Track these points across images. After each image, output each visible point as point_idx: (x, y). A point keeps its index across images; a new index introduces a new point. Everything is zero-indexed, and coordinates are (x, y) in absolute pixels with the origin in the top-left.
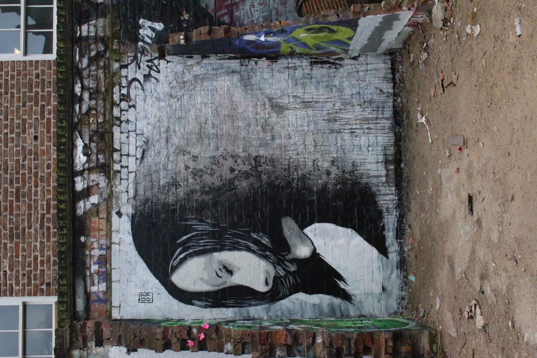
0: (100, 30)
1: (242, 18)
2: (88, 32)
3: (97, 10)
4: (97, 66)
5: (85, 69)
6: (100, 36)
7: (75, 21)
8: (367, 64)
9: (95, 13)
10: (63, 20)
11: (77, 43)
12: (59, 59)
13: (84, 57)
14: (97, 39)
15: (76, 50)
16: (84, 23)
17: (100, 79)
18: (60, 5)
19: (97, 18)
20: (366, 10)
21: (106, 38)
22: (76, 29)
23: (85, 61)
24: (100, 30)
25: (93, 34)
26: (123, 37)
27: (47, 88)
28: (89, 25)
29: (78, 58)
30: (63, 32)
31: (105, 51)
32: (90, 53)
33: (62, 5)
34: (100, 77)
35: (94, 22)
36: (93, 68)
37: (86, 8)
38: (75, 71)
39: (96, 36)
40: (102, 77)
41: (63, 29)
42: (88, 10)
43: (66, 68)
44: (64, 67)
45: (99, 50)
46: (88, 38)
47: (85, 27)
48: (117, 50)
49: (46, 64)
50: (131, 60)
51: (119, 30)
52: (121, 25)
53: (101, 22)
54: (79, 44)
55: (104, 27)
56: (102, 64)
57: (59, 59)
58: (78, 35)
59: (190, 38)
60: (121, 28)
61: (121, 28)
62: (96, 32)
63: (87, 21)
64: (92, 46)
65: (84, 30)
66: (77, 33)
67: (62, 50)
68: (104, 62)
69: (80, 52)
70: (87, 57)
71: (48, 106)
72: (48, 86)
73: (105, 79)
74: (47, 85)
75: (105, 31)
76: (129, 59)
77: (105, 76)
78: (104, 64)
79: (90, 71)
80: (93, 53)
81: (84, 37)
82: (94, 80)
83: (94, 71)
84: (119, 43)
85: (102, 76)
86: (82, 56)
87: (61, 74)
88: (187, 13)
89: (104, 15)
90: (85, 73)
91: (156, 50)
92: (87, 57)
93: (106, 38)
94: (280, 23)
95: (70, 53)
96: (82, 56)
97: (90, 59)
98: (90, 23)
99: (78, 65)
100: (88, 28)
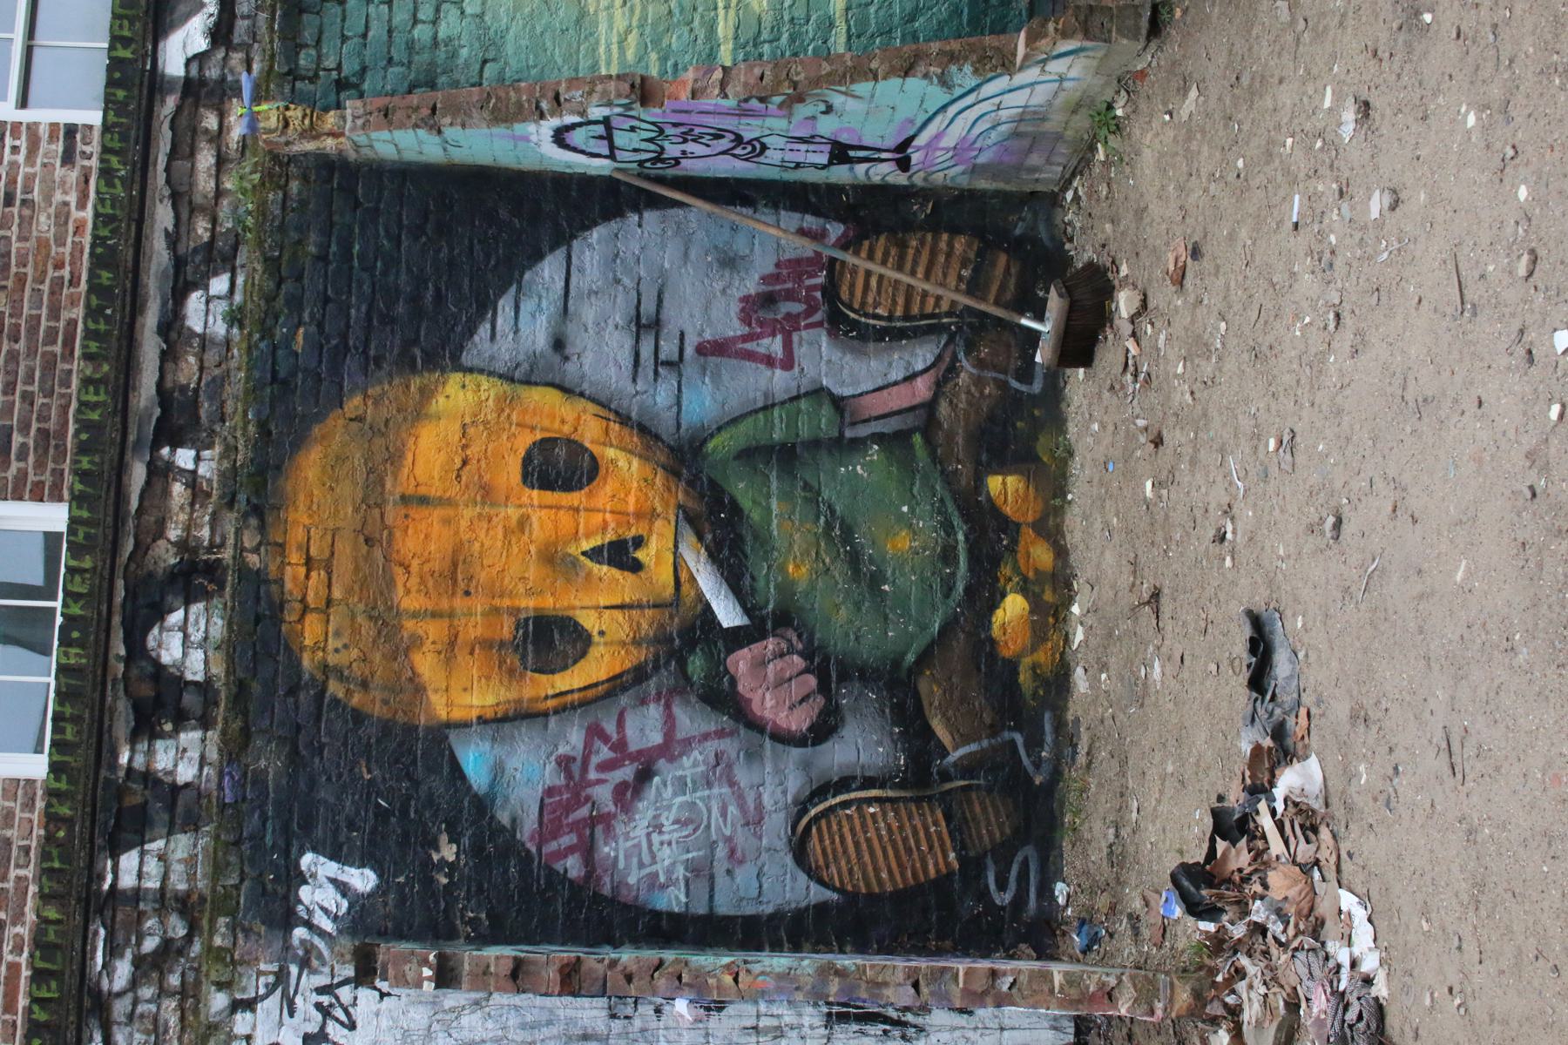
0: (178, 870)
1: (621, 864)
2: (140, 876)
3: (171, 807)
4: (161, 988)
5: (119, 995)
7: (99, 841)
8: (1002, 1029)
9: (166, 817)
10: (61, 834)
11: (100, 911)
12: (42, 958)
13: (122, 956)
14: (164, 900)
15: (96, 933)
17: (166, 1031)
18: (57, 785)
19: (170, 834)
20: (1005, 988)
21: (195, 897)
22: (99, 866)
23: (124, 969)
24: (178, 870)
25: (152, 884)
26: (247, 909)
27: (17, 866)
28: (142, 854)
29: (99, 960)
30: (60, 870)
31: (189, 938)
32: (139, 944)
33: (63, 786)
34: (166, 1022)
35: (160, 844)
36: (147, 992)
37: (138, 799)
38: (87, 1003)
39: (163, 888)
40: (171, 1024)
41: (61, 861)
42: (146, 802)
43: (60, 989)
44: (54, 985)
45: (170, 934)
46: (137, 894)
47: (129, 861)
48: (228, 950)
49: (20, 792)
50: (267, 985)
51: (237, 887)
52: (242, 871)
53: (182, 845)
54: (108, 913)
55: (190, 862)
56: (174, 980)
57: (42, 958)
58: (106, 887)
59: (452, 970)
60: (242, 880)
61: (242, 880)
62: (165, 878)
64: (149, 923)
65: (129, 869)
67: (51, 929)
68: (183, 975)
69: (109, 940)
70: (129, 954)
71: (14, 924)
72: (21, 862)
73: (183, 1029)
74: (17, 858)
75: (191, 877)
76: (262, 980)
77: (182, 1019)
78: (183, 983)
79: (135, 1002)
80: (150, 944)
81: (124, 891)
82: (147, 1033)
83: (149, 1001)
84: (233, 928)
85: (173, 1021)
86: (113, 952)
87: (42, 1008)
88: (450, 842)
89: (192, 824)
90: (120, 1008)
91: (348, 957)
92: (129, 954)
93: (195, 897)
94: (736, 980)
95: (78, 945)
96: (113, 952)
97: (138, 961)
98: (147, 847)
99: (98, 982)
100: (141, 863)
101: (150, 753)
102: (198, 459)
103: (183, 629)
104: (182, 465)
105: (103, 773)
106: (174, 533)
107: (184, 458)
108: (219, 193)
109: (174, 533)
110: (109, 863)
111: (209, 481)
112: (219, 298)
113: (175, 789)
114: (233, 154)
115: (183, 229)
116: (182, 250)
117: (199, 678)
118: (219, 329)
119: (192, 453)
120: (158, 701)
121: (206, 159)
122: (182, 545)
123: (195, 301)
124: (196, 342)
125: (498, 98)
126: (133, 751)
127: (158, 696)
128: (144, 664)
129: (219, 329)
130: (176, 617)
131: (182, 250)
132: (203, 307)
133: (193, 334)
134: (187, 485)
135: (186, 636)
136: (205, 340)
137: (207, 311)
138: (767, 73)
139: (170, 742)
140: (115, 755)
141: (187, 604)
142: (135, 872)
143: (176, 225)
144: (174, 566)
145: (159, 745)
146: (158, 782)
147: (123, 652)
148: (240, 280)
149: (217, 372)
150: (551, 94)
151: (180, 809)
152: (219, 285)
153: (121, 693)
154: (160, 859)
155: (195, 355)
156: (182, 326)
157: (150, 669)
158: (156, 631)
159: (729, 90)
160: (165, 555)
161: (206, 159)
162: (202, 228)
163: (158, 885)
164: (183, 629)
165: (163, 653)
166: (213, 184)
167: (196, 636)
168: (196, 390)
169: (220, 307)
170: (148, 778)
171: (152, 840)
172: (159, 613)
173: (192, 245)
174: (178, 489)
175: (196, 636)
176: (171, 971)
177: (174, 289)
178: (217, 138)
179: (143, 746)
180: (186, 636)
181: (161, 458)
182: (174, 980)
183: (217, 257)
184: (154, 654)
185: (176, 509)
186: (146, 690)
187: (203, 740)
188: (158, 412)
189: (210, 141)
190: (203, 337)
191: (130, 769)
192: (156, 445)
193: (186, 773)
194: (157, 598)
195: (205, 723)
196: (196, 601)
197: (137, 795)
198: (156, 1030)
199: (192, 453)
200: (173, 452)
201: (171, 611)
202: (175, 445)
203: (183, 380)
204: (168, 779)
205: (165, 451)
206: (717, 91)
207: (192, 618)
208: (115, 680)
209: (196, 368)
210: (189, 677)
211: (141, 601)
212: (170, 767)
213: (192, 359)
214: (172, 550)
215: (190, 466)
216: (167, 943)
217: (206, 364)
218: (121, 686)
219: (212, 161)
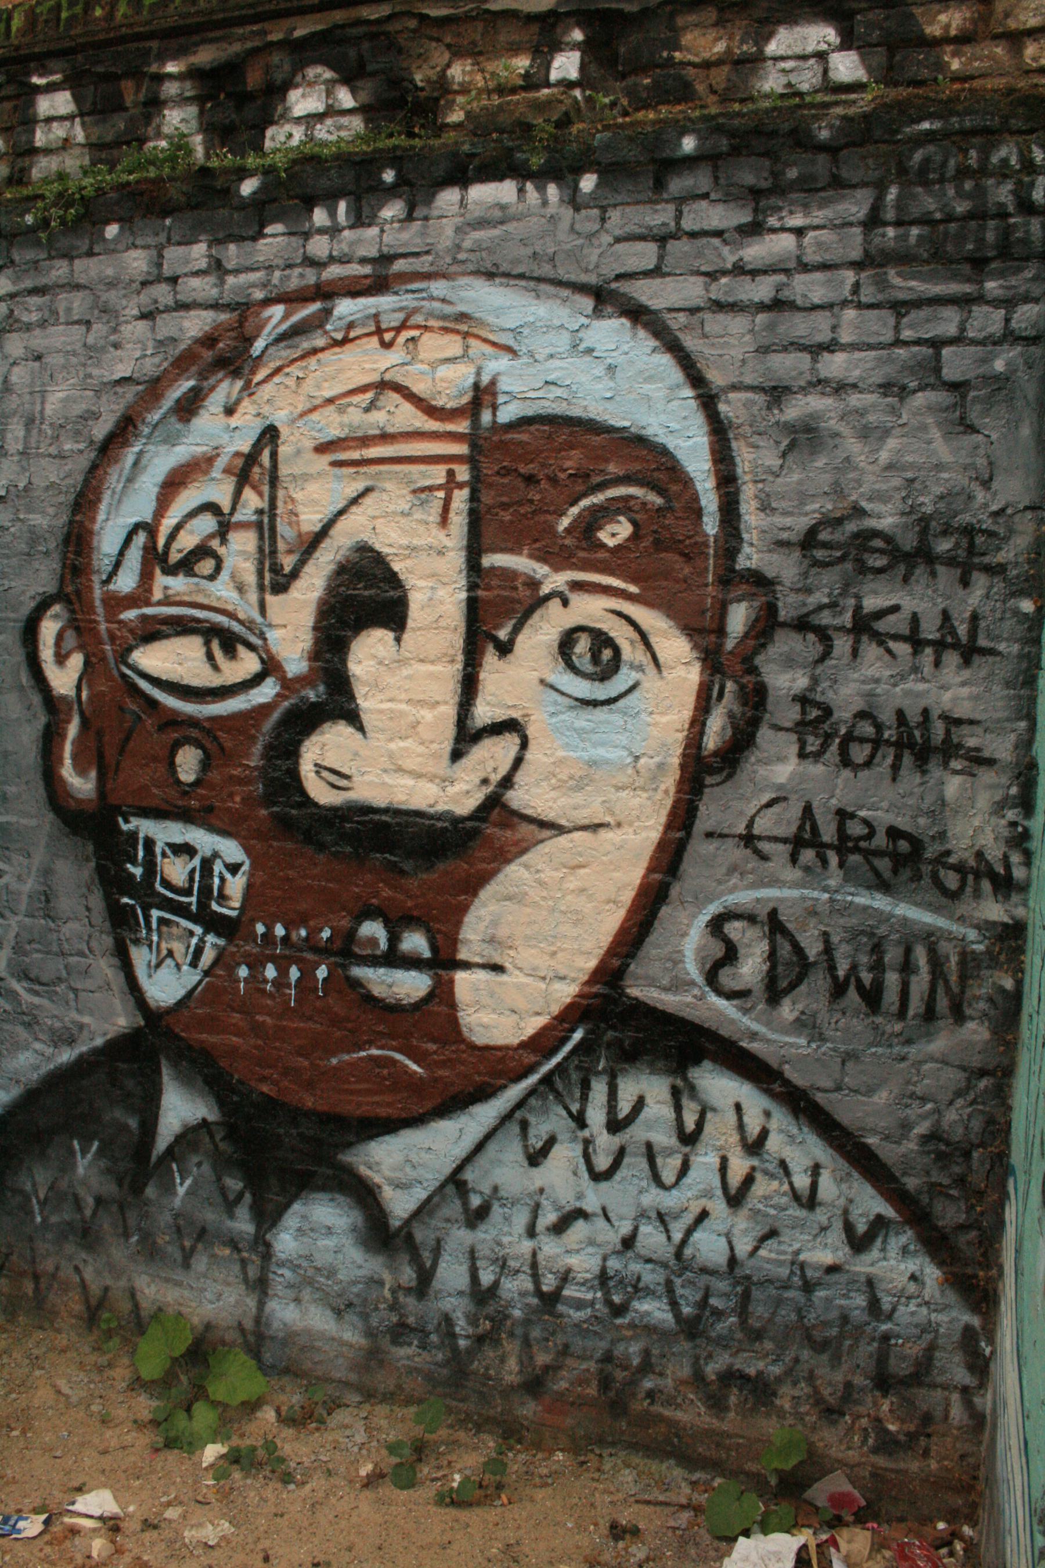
2: (49, 120)
9: (109, 138)
16: (77, 99)
22: (52, 64)
25: (40, 138)
28: (70, 118)
37: (129, 100)
42: (122, 108)
47: (62, 102)
62: (47, 151)
63: (84, 111)
66: (41, 76)
98: (78, 120)
100: (62, 118)
101: (182, 101)
103: (331, 111)
104: (556, 64)
105: (155, 44)
106: (458, 72)
107: (566, 65)
109: (458, 72)
110: (57, 77)
112: (826, 71)
119: (574, 74)
120: (242, 99)
122: (442, 86)
123: (821, 34)
126: (180, 77)
128: (287, 67)
129: (771, 82)
130: (345, 98)
132: (810, 49)
134: (527, 76)
135: (320, 117)
137: (804, 58)
139: (194, 124)
140: (174, 58)
141: (362, 110)
142: (53, 113)
144: (412, 81)
146: (148, 118)
147: (298, 33)
149: (700, 88)
152: (846, 67)
153: (249, 45)
154: (66, 140)
155: (729, 50)
156: (779, 22)
158: (328, 74)
163: (38, 144)
164: (331, 111)
165: (299, 91)
168: (670, 62)
169: (807, 79)
170: (155, 104)
174: (522, 63)
175: (321, 132)
179: (189, 89)
181: (567, 30)
184: (298, 78)
185: (490, 67)
186: (254, 79)
191: (161, 78)
192: (584, 18)
194: (370, 68)
196: (367, 121)
197: (131, 93)
199: (574, 74)
200: (575, 46)
201: (354, 92)
202: (586, 48)
203: (687, 39)
205: (578, 35)
207: (344, 120)
208: (265, 33)
209: (706, 55)
211: (366, 45)
213: (720, 47)
214: (433, 74)
215: (554, 76)
217: (713, 71)
218: (257, 43)
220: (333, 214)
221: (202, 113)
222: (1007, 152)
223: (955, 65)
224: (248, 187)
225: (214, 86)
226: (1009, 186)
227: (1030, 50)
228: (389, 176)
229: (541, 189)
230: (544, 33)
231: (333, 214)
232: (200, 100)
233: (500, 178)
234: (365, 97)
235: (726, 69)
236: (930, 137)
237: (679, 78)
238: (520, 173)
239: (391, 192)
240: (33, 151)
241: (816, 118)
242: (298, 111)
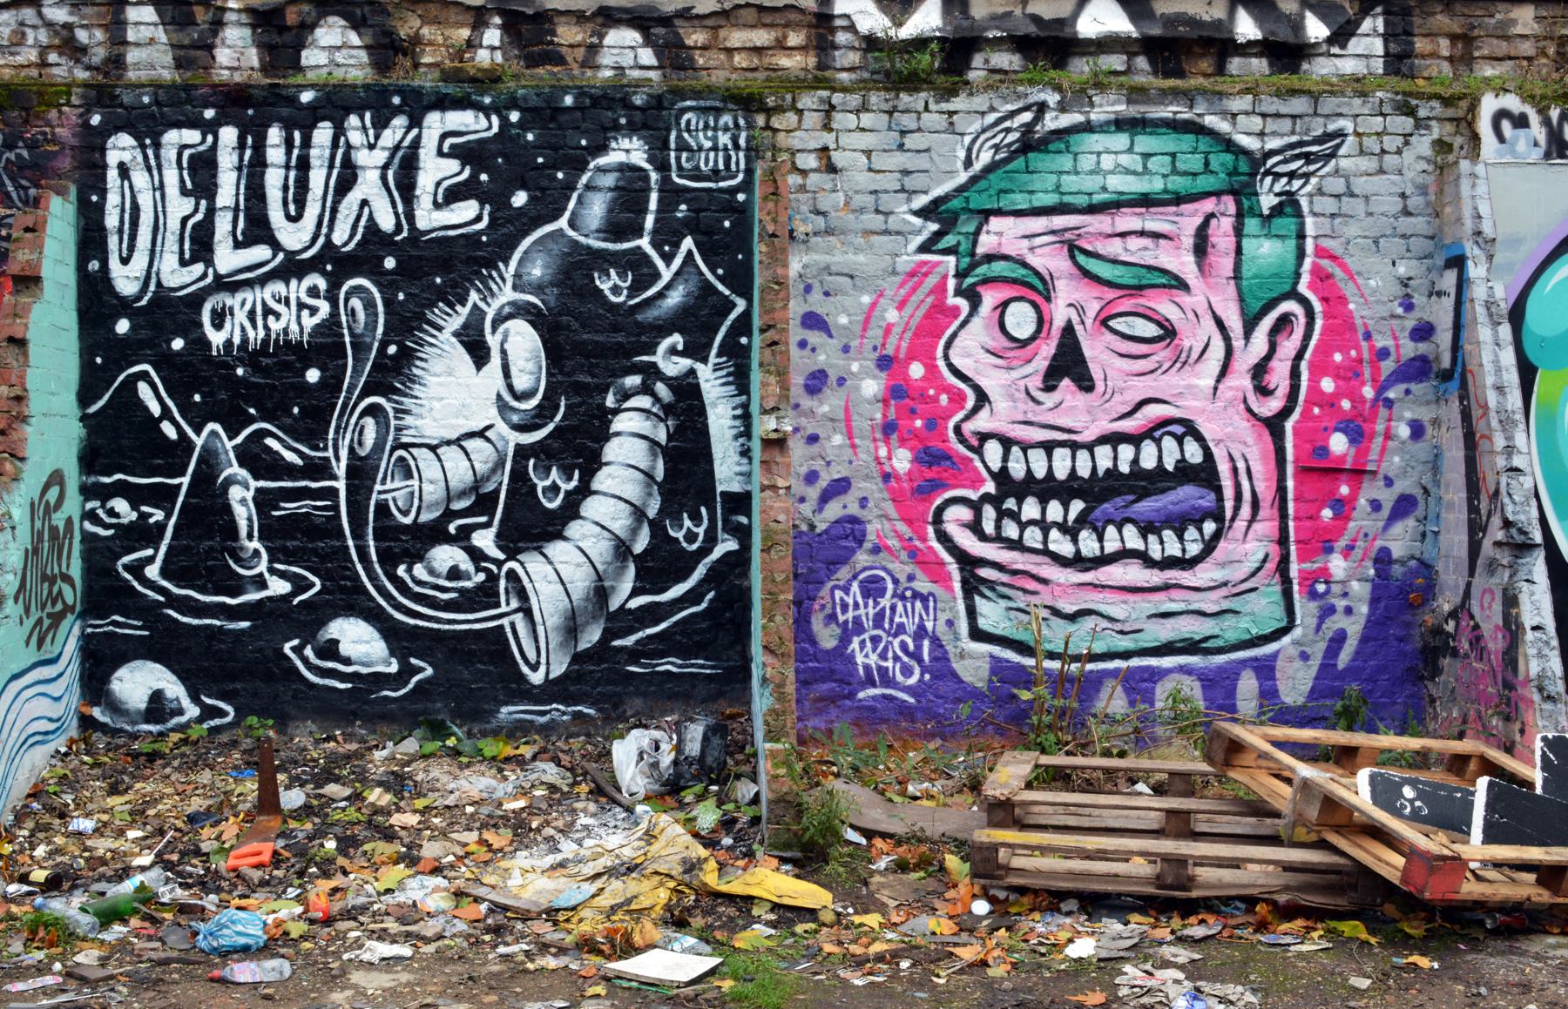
2: (136, 24)
3: (194, 46)
5: (40, 14)
6: (124, 55)
9: (186, 42)
13: (71, 14)
16: (159, 13)
17: (12, 54)
19: (172, 45)
25: (131, 35)
28: (156, 25)
32: (82, 26)
35: (163, 38)
36: (43, 36)
47: (148, 13)
62: (137, 45)
65: (142, 16)
68: (58, 65)
79: (34, 27)
80: (82, 36)
81: (123, 12)
85: (20, 59)
89: (179, 64)
92: (71, 19)
97: (68, 27)
102: (493, 48)
103: (345, 46)
104: (486, 36)
106: (425, 31)
107: (492, 36)
108: (730, 51)
111: (472, 59)
113: (210, 48)
114: (767, 60)
115: (696, 22)
116: (677, 22)
117: (304, 62)
118: (607, 59)
119: (497, 44)
120: (283, 29)
121: (761, 37)
122: (416, 40)
123: (632, 36)
124: (595, 40)
125: (777, 293)
127: (289, 29)
128: (314, 14)
130: (354, 38)
131: (677, 22)
133: (602, 36)
135: (339, 48)
136: (593, 49)
138: (780, 526)
139: (249, 41)
141: (367, 47)
143: (698, 17)
145: (247, 32)
146: (215, 34)
148: (653, 74)
149: (569, 59)
150: (776, 338)
151: (192, 53)
157: (309, 20)
158: (343, 22)
159: (768, 493)
160: (408, 25)
161: (761, 37)
162: (696, 38)
164: (345, 46)
166: (737, 45)
167: (339, 57)
168: (552, 43)
169: (627, 60)
170: (218, 24)
171: (166, 31)
172: (356, 25)
173: (681, 31)
175: (339, 57)
176: (60, 54)
177: (641, 18)
178: (780, 45)
179: (244, 18)
180: (339, 48)
182: (53, 57)
183: (673, 55)
187: (252, 69)
188: (530, 11)
189: (777, 39)
190: (600, 45)
192: (502, 12)
193: (223, 56)
195: (265, 69)
196: (370, 55)
198: (13, 45)
199: (497, 44)
201: (360, 35)
202: (505, 28)
203: (560, 30)
204: (218, 41)
205: (497, 20)
206: (766, 482)
210: (304, 53)
211: (366, 9)
212: (228, 42)
213: (579, 38)
215: (485, 43)
216: (84, 50)
219: (758, 44)
220: (362, 119)
221: (254, 33)
222: (726, 119)
223: (701, 61)
224: (306, 97)
225: (263, 21)
226: (729, 135)
227: (737, 58)
228: (396, 100)
229: (488, 118)
230: (479, 19)
231: (362, 119)
232: (254, 26)
233: (464, 108)
234: (369, 40)
235: (582, 49)
236: (690, 109)
237: (558, 53)
238: (478, 107)
239: (397, 111)
240: (125, 43)
241: (635, 93)
242: (323, 43)
